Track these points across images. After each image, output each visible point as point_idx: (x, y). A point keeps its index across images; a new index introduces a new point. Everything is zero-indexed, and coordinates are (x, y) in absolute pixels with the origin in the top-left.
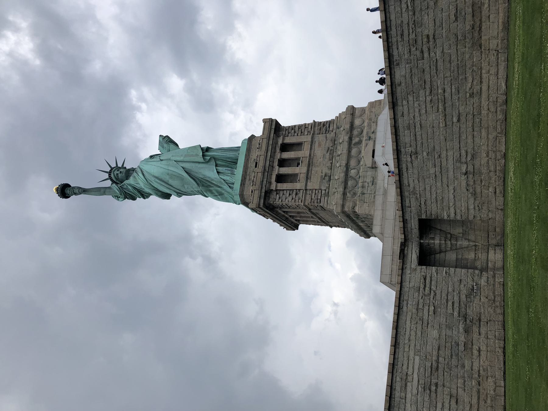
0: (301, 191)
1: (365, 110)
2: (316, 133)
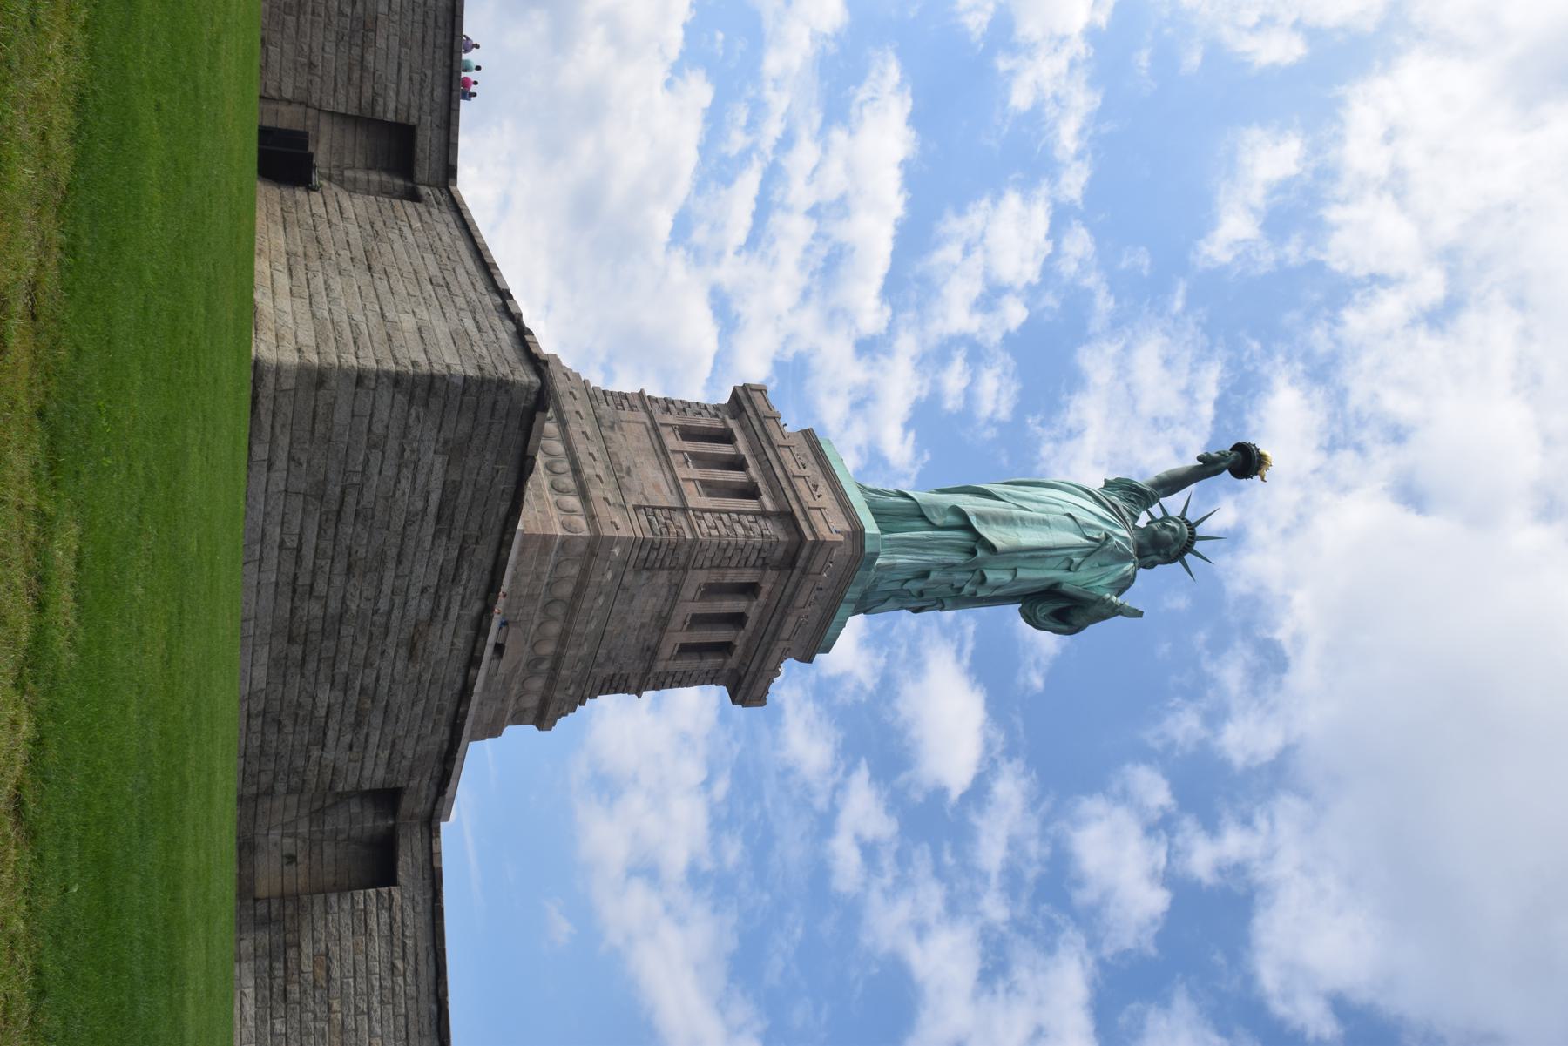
1: (564, 527)
2: (677, 516)
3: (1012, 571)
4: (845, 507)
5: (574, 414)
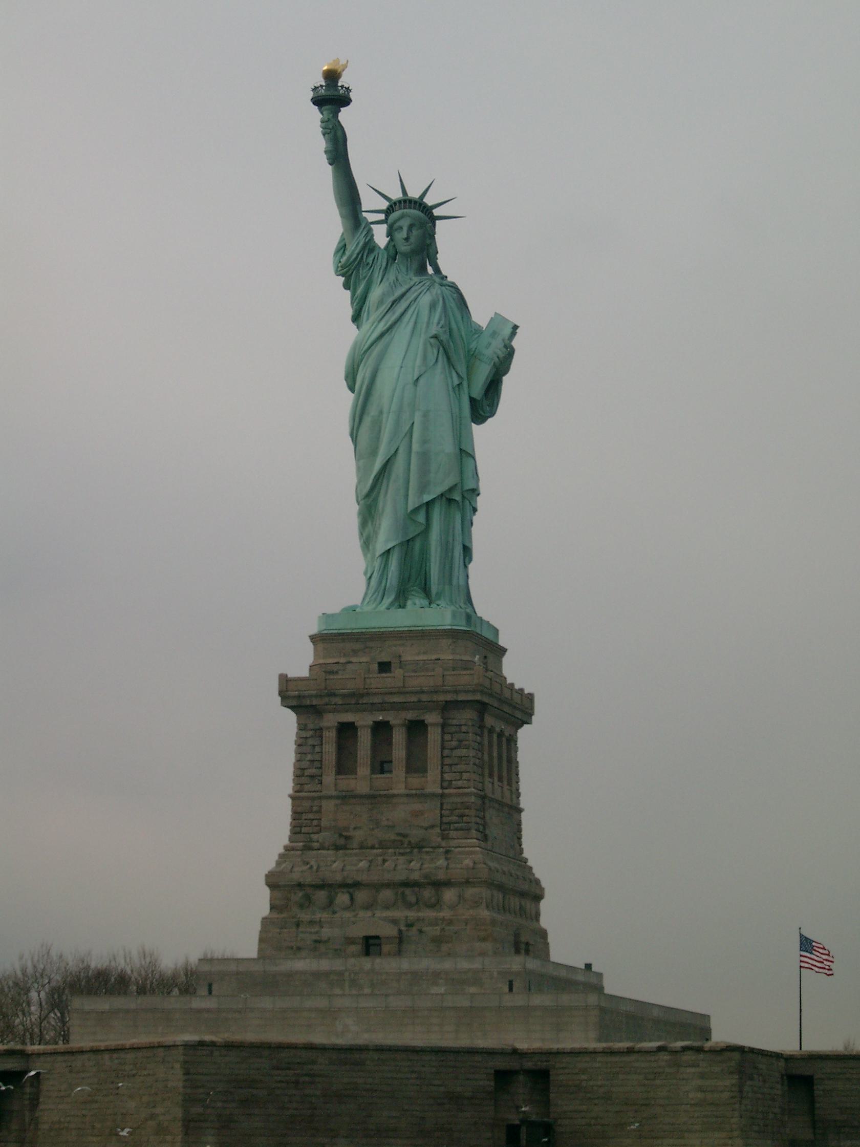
0: (318, 787)
1: (478, 906)
3: (464, 455)
4: (422, 636)
5: (345, 873)
